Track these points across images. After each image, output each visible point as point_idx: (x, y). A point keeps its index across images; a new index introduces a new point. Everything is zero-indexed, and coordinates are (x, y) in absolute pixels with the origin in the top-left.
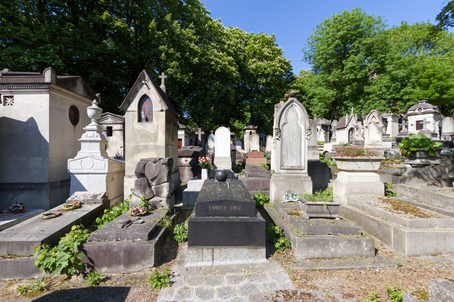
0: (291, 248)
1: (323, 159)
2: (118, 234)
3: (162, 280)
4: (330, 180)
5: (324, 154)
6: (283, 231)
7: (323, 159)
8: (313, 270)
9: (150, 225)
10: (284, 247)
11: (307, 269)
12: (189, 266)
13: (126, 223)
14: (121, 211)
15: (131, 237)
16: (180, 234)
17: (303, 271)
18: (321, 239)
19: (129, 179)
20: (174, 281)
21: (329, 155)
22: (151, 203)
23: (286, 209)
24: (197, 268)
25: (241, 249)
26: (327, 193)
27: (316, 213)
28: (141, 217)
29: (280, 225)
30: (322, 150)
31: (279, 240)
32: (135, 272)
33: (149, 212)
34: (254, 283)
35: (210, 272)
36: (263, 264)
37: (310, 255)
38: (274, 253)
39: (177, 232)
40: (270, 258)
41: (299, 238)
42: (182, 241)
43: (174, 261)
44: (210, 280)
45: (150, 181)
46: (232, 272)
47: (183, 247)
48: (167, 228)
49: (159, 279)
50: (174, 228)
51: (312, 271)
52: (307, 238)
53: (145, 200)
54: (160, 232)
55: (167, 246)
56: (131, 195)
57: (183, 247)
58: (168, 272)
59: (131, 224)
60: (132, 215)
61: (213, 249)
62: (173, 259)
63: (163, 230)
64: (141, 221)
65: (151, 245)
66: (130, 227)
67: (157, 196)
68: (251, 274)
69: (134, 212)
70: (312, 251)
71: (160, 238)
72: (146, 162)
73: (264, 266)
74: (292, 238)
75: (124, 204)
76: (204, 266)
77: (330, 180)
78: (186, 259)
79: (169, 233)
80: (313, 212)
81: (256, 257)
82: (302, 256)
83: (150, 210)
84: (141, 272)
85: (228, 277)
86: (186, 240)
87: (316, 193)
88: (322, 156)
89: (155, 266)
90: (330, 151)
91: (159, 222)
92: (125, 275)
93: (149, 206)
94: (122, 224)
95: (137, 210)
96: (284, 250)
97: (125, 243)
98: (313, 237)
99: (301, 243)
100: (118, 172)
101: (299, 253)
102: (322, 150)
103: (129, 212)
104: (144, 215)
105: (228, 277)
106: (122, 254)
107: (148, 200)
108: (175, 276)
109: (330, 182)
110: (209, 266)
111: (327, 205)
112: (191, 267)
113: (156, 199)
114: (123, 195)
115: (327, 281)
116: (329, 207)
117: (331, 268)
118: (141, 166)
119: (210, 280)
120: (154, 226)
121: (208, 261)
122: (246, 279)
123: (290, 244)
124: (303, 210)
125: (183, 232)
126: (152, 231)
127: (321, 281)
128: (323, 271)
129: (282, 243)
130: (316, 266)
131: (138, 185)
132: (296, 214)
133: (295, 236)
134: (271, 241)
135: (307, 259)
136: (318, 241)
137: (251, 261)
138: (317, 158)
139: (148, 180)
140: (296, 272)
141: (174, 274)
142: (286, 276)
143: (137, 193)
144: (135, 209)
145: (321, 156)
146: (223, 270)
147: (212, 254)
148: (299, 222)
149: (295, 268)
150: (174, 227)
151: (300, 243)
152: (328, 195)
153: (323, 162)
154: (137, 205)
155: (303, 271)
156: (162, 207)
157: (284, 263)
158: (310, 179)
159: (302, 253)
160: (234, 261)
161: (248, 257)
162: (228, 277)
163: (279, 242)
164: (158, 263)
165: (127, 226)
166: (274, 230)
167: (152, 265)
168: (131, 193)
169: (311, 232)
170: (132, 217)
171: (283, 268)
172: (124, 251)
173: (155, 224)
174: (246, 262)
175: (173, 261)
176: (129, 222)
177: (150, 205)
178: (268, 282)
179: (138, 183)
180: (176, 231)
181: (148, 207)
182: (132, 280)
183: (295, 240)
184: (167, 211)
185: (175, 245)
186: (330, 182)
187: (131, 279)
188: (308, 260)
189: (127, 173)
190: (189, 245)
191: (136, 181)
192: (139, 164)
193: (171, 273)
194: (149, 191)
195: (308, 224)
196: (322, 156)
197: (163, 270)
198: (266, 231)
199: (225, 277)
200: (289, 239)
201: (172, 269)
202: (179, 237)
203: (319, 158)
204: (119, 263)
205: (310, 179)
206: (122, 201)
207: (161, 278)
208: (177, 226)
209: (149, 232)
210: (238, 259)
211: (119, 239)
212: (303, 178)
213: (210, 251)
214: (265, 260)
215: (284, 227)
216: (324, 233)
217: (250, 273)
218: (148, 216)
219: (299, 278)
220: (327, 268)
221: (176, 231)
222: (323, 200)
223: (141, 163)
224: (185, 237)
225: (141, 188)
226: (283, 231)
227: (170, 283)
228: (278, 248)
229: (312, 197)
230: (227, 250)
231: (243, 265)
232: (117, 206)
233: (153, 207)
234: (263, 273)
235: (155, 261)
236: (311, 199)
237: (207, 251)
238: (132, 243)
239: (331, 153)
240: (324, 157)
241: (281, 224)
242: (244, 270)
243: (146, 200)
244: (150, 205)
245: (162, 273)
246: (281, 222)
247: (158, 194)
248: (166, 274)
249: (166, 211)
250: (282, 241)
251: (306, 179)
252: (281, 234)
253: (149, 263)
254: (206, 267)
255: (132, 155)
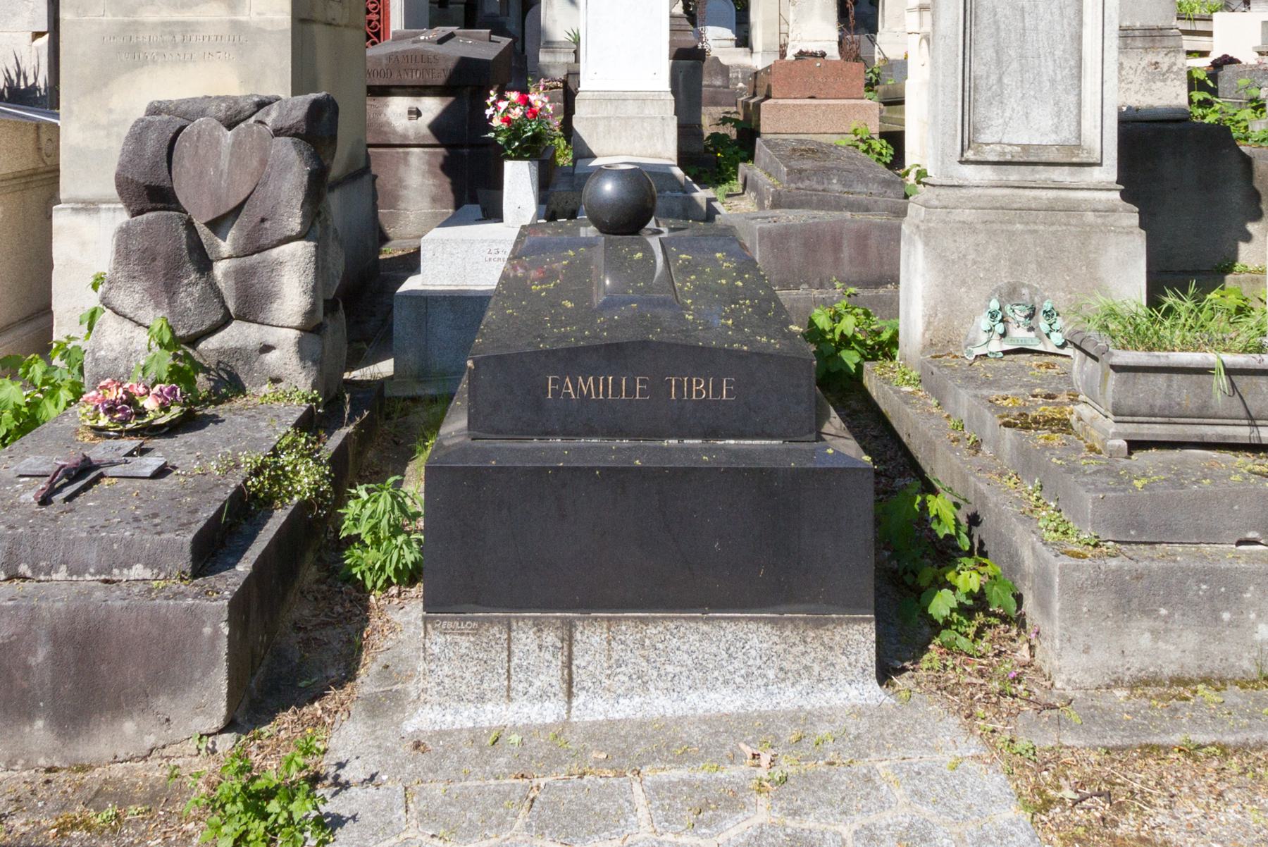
0: (1021, 622)
1: (1206, 104)
2: (16, 541)
3: (273, 806)
4: (1252, 227)
5: (1213, 76)
6: (974, 520)
7: (1206, 104)
8: (1152, 747)
9: (202, 488)
10: (980, 618)
11: (1116, 741)
12: (426, 726)
13: (67, 474)
14: (34, 405)
15: (92, 556)
16: (377, 542)
17: (1093, 757)
18: (1196, 572)
19: (82, 220)
20: (346, 813)
21: (1243, 82)
22: (211, 362)
23: (994, 393)
24: (475, 736)
25: (730, 628)
26: (1232, 301)
27: (1169, 415)
28: (149, 444)
29: (958, 488)
30: (1204, 54)
31: (950, 576)
32: (115, 760)
33: (199, 411)
34: (810, 823)
35: (553, 760)
36: (860, 714)
37: (1135, 665)
38: (924, 649)
39: (363, 529)
40: (901, 682)
41: (1067, 561)
42: (388, 583)
43: (341, 695)
44: (554, 806)
45: (204, 233)
46: (679, 761)
47: (396, 617)
48: (304, 506)
49: (256, 801)
50: (343, 504)
51: (1144, 756)
52: (1113, 563)
53: (176, 342)
54: (260, 525)
55: (302, 611)
56: (93, 314)
57: (396, 617)
58: (310, 760)
59: (96, 480)
60: (99, 431)
61: (570, 626)
62: (340, 685)
63: (279, 517)
64: (151, 463)
65: (211, 607)
66: (88, 501)
67: (243, 317)
68: (792, 770)
69: (110, 411)
70: (1146, 640)
71: (259, 566)
72: (179, 122)
73: (864, 724)
74: (1029, 562)
75: (50, 368)
76: (515, 728)
77: (1252, 227)
78: (412, 688)
79: (315, 534)
80: (1153, 414)
81: (819, 672)
82: (1087, 670)
83: (206, 401)
84: (153, 762)
85: (657, 788)
86: (410, 576)
87: (1170, 300)
88: (1202, 86)
89: (230, 725)
90: (1248, 57)
91: (257, 472)
92: (62, 777)
93: (201, 378)
94: (43, 484)
95: (131, 400)
96: (979, 634)
97: (59, 590)
98: (1147, 559)
99: (1081, 590)
100: (15, 177)
101: (1070, 652)
102: (1204, 54)
103: (83, 412)
104: (172, 429)
105: (656, 789)
106: (40, 655)
107: (193, 341)
108: (346, 786)
109: (1248, 238)
110: (545, 728)
111: (1230, 372)
112: (442, 734)
113: (238, 335)
114: (45, 311)
115: (1232, 814)
116: (1241, 381)
117: (1254, 737)
118: (153, 144)
119: (554, 806)
120: (224, 494)
121: (543, 696)
122: (763, 800)
123: (1019, 599)
124: (1094, 399)
125: (396, 530)
126: (213, 522)
127: (1198, 812)
128: (1210, 756)
129: (970, 594)
130: (1167, 724)
131: (136, 256)
132: (1049, 422)
133: (1048, 554)
134: (909, 579)
135: (1118, 683)
136: (1181, 582)
137: (789, 698)
138: (1171, 95)
139: (190, 225)
140: (1053, 761)
141: (345, 775)
142: (995, 781)
143: (127, 299)
144: (115, 394)
145: (1194, 84)
146: (628, 749)
147: (561, 658)
148: (1071, 471)
149: (1047, 740)
150: (341, 499)
151: (1075, 591)
152: (1240, 310)
153: (1211, 119)
154: (129, 373)
155: (1093, 757)
156: (276, 380)
157: (980, 710)
158: (1130, 217)
159: (1087, 650)
160: (693, 697)
161: (771, 674)
162: (656, 789)
163: (954, 588)
164: (254, 702)
165: (68, 491)
166: (924, 519)
167: (218, 722)
168: (93, 300)
169: (1136, 526)
170: (102, 443)
171: (974, 741)
172: (54, 637)
173: (234, 482)
174: (759, 701)
175: (335, 697)
176: (84, 473)
177: (207, 370)
178: (887, 817)
179: (135, 244)
180: (356, 520)
181: (190, 383)
182: (99, 810)
183: (1043, 576)
184: (305, 406)
185: (348, 605)
186: (1248, 238)
187: (96, 799)
188: (1121, 694)
189: (68, 186)
190: (432, 605)
191: (125, 234)
192: (139, 134)
193: (326, 766)
194: (196, 291)
195: (1125, 482)
196: (1202, 86)
197: (276, 749)
198: (878, 522)
199: (637, 788)
200: (1013, 566)
201: (333, 743)
202: (372, 556)
203: (1183, 100)
204: (22, 709)
205: (1134, 219)
206: (43, 345)
207: (269, 794)
208: (362, 491)
209: (196, 528)
210: (713, 688)
211: (24, 569)
212: (1090, 217)
213: (550, 638)
214: (871, 692)
215: (983, 498)
216: (1212, 536)
217: (786, 766)
218: (192, 437)
219: (1068, 794)
220: (1230, 739)
221: (356, 520)
222: (1210, 343)
223: (148, 126)
224: (409, 558)
225: (149, 272)
226: (974, 520)
227: (320, 822)
228: (948, 624)
229: (1144, 323)
230: (651, 630)
231: (742, 719)
232: (14, 377)
233: (219, 382)
234: (860, 767)
235: (230, 695)
236: (1136, 338)
237: (532, 641)
238: (99, 594)
239: (1253, 70)
240: (1214, 92)
241: (965, 479)
242: (748, 751)
243: (183, 343)
244: (207, 370)
245: (272, 765)
246: (967, 471)
247: (252, 305)
248: (295, 775)
249: (298, 409)
250: (968, 579)
251: (1112, 218)
252: (964, 543)
253: (200, 709)
254: (528, 731)
255: (101, 81)
